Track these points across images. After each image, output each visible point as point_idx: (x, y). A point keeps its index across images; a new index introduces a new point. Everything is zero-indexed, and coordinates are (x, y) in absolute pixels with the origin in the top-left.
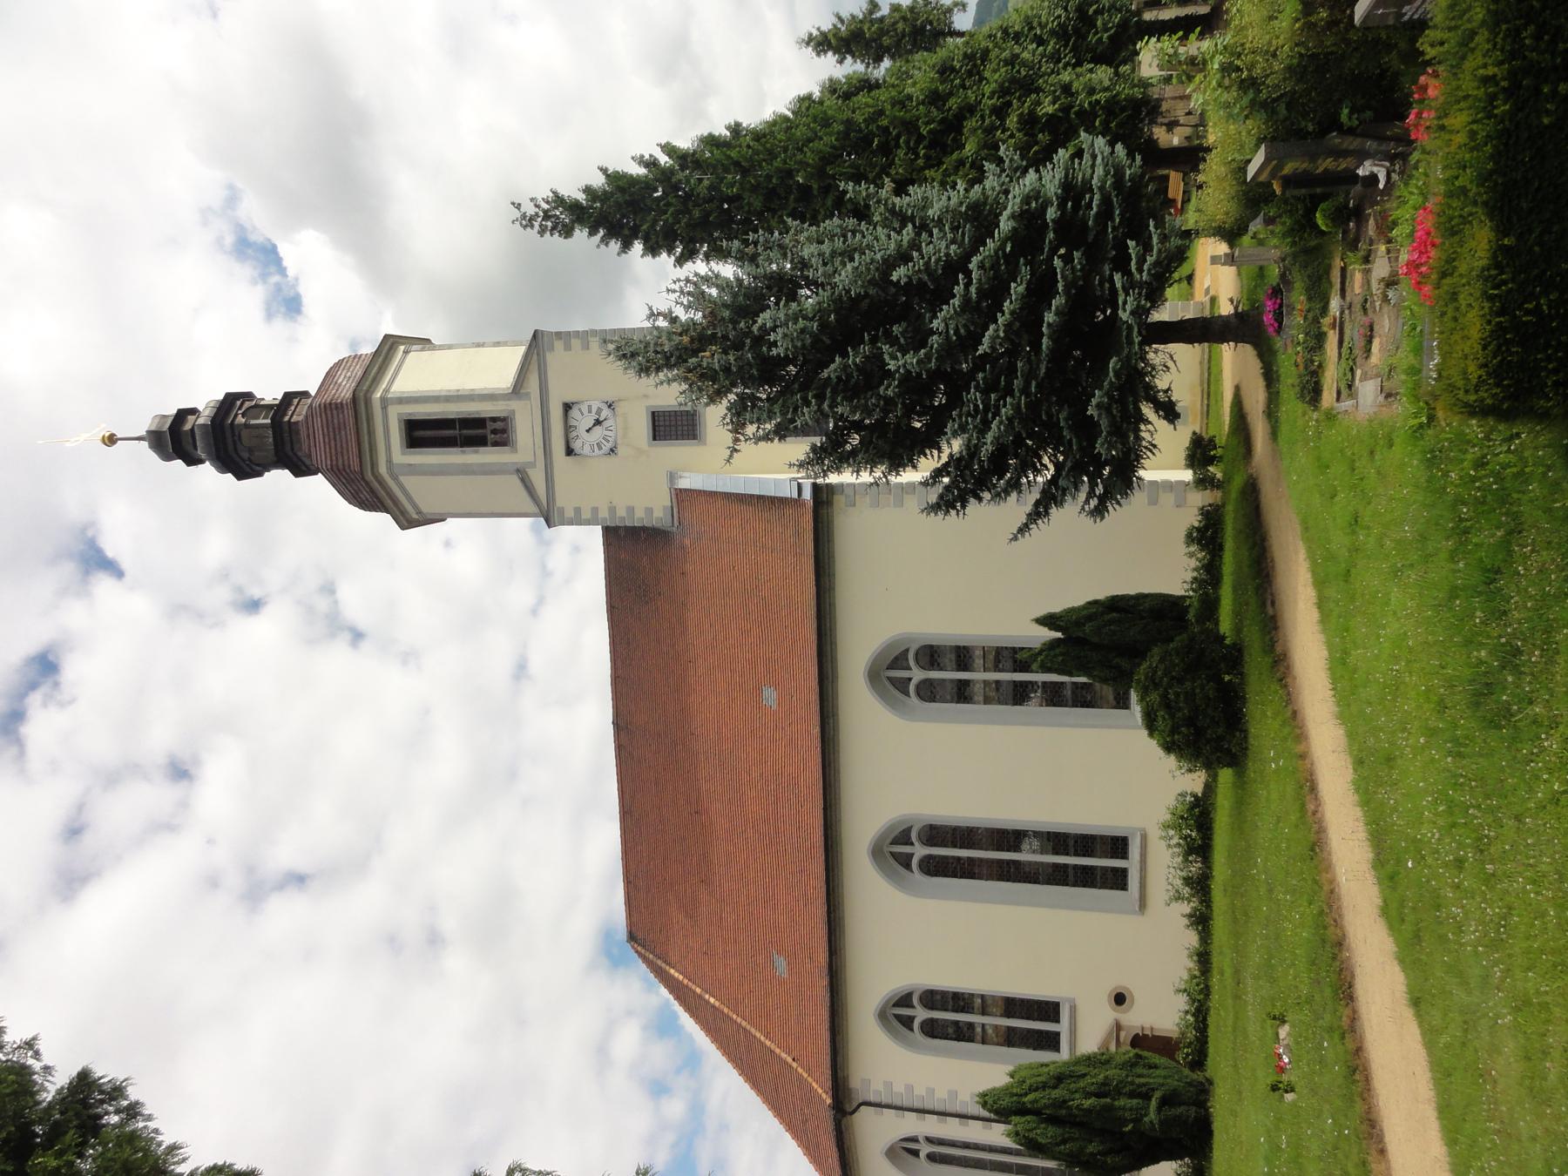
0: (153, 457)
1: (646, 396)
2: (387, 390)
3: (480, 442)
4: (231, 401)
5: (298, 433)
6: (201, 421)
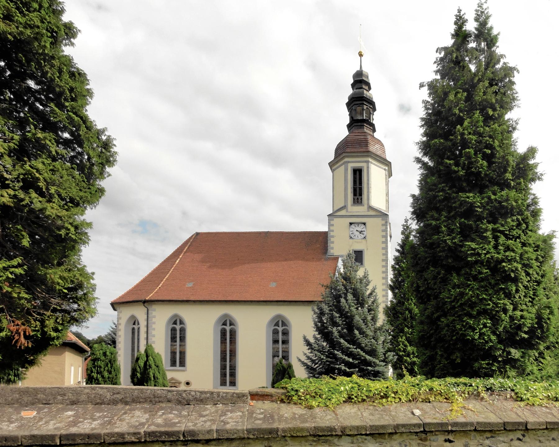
0: (354, 72)
2: (371, 163)
3: (355, 194)
4: (371, 103)
5: (360, 128)
6: (365, 92)
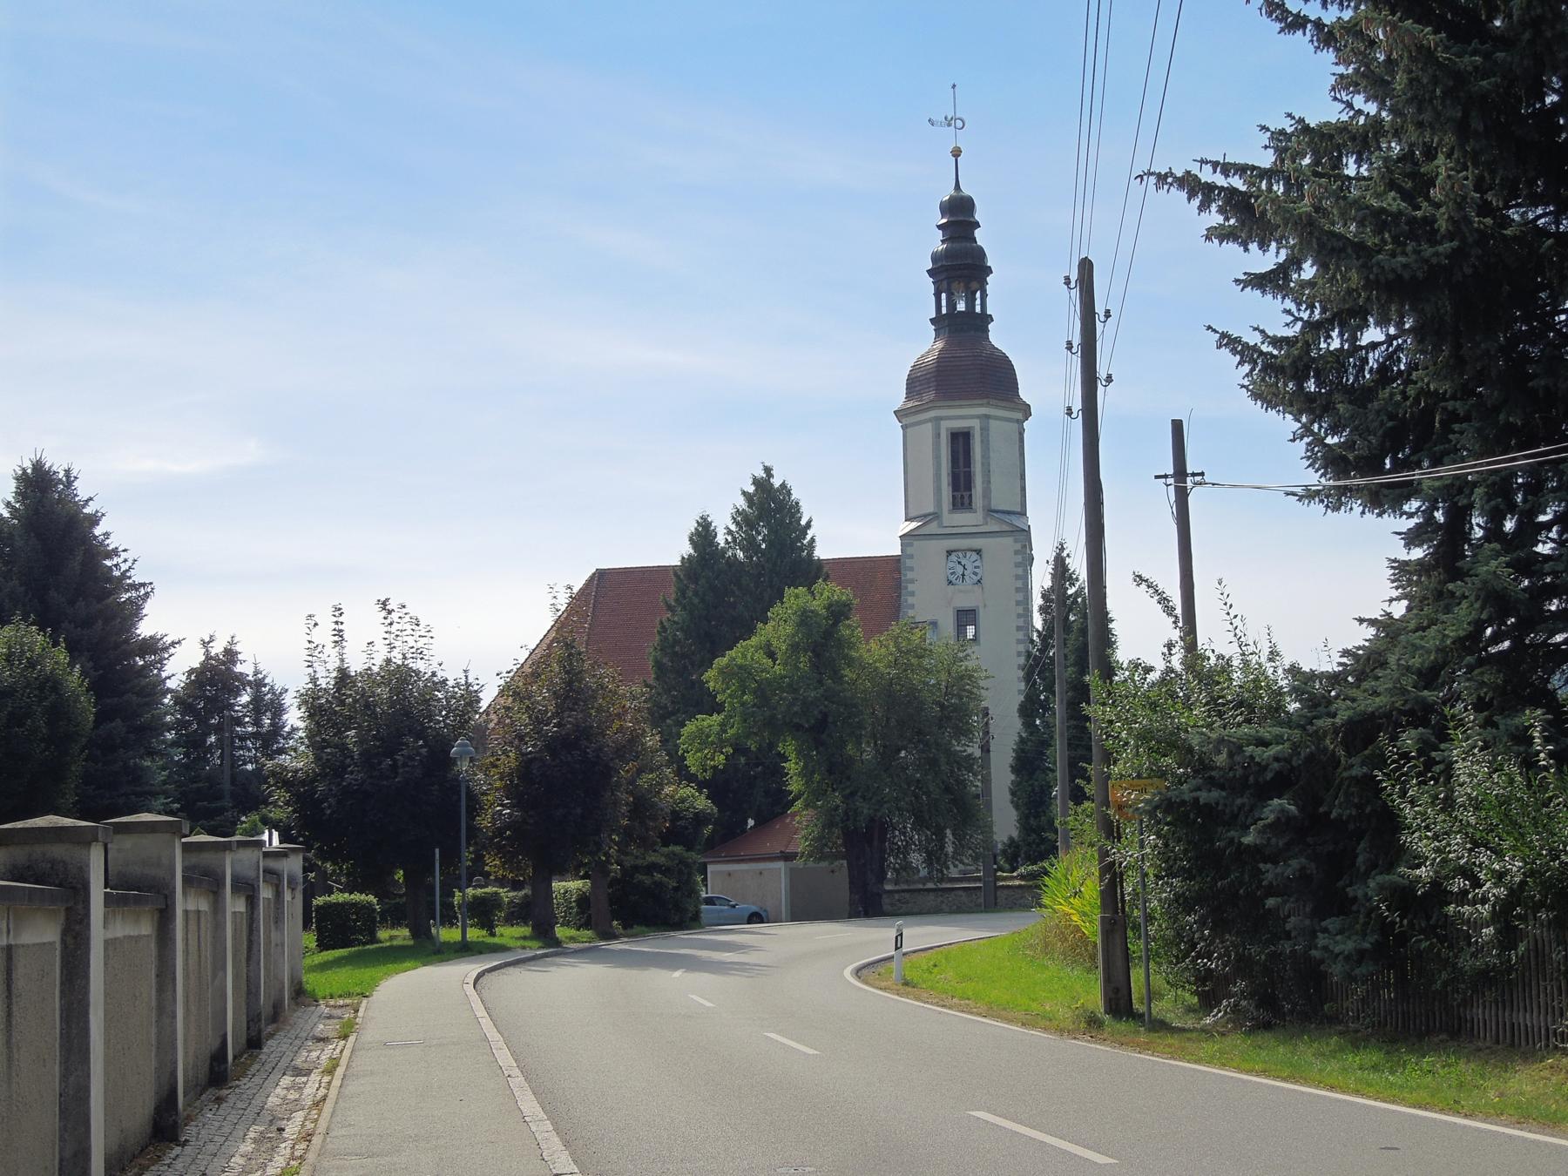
1: (985, 606)
